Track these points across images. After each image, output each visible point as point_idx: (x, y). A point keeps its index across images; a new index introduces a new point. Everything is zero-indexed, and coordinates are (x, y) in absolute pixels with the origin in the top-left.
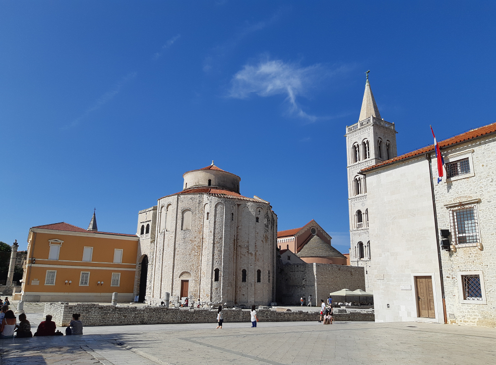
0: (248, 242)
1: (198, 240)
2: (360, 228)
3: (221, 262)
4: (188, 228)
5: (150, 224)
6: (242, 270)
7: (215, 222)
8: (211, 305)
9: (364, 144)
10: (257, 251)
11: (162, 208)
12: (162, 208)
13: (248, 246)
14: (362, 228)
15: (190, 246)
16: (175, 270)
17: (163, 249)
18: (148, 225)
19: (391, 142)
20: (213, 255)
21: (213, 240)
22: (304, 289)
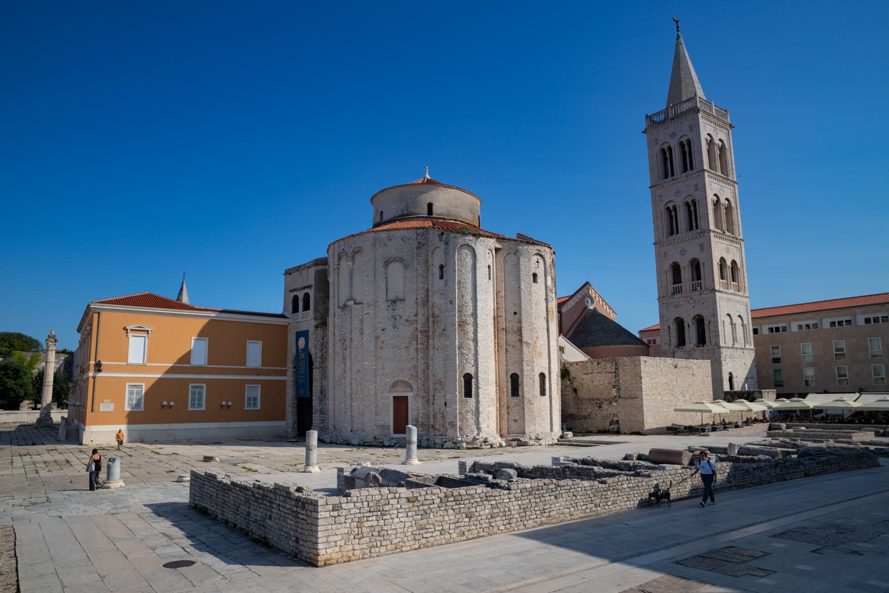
1: (421, 319)
5: (311, 292)
6: (509, 374)
9: (682, 145)
10: (537, 338)
11: (339, 259)
12: (339, 259)
15: (406, 331)
17: (351, 339)
18: (307, 297)
19: (725, 142)
22: (614, 404)
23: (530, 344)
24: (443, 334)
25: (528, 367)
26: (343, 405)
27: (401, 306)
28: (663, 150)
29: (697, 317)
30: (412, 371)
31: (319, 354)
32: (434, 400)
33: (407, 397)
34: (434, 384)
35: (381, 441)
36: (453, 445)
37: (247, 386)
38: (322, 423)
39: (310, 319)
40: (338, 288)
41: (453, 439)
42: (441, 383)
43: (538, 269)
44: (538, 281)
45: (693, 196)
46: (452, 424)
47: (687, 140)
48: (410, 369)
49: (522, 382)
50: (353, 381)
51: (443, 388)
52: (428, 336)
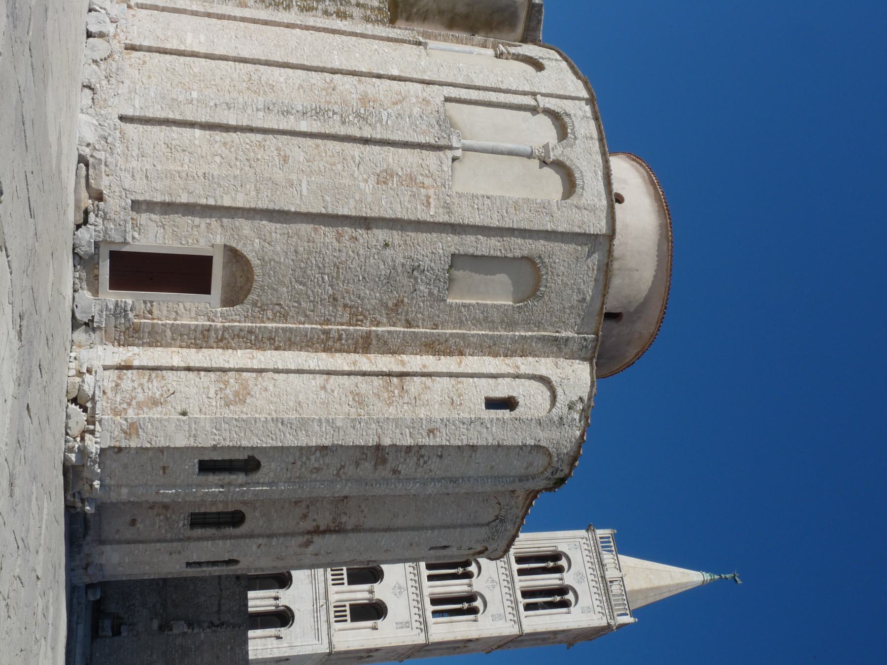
0: (357, 529)
2: (330, 582)
6: (243, 509)
8: (83, 452)
9: (562, 590)
11: (556, 117)
12: (556, 117)
13: (339, 530)
14: (333, 589)
17: (366, 141)
22: (155, 624)
25: (254, 547)
26: (195, 95)
28: (556, 556)
29: (289, 613)
30: (277, 307)
32: (199, 370)
33: (207, 290)
34: (240, 370)
35: (92, 217)
41: (92, 432)
42: (241, 397)
43: (455, 549)
44: (431, 552)
45: (484, 611)
47: (570, 600)
48: (280, 305)
49: (224, 538)
50: (260, 137)
51: (227, 405)
52: (355, 352)
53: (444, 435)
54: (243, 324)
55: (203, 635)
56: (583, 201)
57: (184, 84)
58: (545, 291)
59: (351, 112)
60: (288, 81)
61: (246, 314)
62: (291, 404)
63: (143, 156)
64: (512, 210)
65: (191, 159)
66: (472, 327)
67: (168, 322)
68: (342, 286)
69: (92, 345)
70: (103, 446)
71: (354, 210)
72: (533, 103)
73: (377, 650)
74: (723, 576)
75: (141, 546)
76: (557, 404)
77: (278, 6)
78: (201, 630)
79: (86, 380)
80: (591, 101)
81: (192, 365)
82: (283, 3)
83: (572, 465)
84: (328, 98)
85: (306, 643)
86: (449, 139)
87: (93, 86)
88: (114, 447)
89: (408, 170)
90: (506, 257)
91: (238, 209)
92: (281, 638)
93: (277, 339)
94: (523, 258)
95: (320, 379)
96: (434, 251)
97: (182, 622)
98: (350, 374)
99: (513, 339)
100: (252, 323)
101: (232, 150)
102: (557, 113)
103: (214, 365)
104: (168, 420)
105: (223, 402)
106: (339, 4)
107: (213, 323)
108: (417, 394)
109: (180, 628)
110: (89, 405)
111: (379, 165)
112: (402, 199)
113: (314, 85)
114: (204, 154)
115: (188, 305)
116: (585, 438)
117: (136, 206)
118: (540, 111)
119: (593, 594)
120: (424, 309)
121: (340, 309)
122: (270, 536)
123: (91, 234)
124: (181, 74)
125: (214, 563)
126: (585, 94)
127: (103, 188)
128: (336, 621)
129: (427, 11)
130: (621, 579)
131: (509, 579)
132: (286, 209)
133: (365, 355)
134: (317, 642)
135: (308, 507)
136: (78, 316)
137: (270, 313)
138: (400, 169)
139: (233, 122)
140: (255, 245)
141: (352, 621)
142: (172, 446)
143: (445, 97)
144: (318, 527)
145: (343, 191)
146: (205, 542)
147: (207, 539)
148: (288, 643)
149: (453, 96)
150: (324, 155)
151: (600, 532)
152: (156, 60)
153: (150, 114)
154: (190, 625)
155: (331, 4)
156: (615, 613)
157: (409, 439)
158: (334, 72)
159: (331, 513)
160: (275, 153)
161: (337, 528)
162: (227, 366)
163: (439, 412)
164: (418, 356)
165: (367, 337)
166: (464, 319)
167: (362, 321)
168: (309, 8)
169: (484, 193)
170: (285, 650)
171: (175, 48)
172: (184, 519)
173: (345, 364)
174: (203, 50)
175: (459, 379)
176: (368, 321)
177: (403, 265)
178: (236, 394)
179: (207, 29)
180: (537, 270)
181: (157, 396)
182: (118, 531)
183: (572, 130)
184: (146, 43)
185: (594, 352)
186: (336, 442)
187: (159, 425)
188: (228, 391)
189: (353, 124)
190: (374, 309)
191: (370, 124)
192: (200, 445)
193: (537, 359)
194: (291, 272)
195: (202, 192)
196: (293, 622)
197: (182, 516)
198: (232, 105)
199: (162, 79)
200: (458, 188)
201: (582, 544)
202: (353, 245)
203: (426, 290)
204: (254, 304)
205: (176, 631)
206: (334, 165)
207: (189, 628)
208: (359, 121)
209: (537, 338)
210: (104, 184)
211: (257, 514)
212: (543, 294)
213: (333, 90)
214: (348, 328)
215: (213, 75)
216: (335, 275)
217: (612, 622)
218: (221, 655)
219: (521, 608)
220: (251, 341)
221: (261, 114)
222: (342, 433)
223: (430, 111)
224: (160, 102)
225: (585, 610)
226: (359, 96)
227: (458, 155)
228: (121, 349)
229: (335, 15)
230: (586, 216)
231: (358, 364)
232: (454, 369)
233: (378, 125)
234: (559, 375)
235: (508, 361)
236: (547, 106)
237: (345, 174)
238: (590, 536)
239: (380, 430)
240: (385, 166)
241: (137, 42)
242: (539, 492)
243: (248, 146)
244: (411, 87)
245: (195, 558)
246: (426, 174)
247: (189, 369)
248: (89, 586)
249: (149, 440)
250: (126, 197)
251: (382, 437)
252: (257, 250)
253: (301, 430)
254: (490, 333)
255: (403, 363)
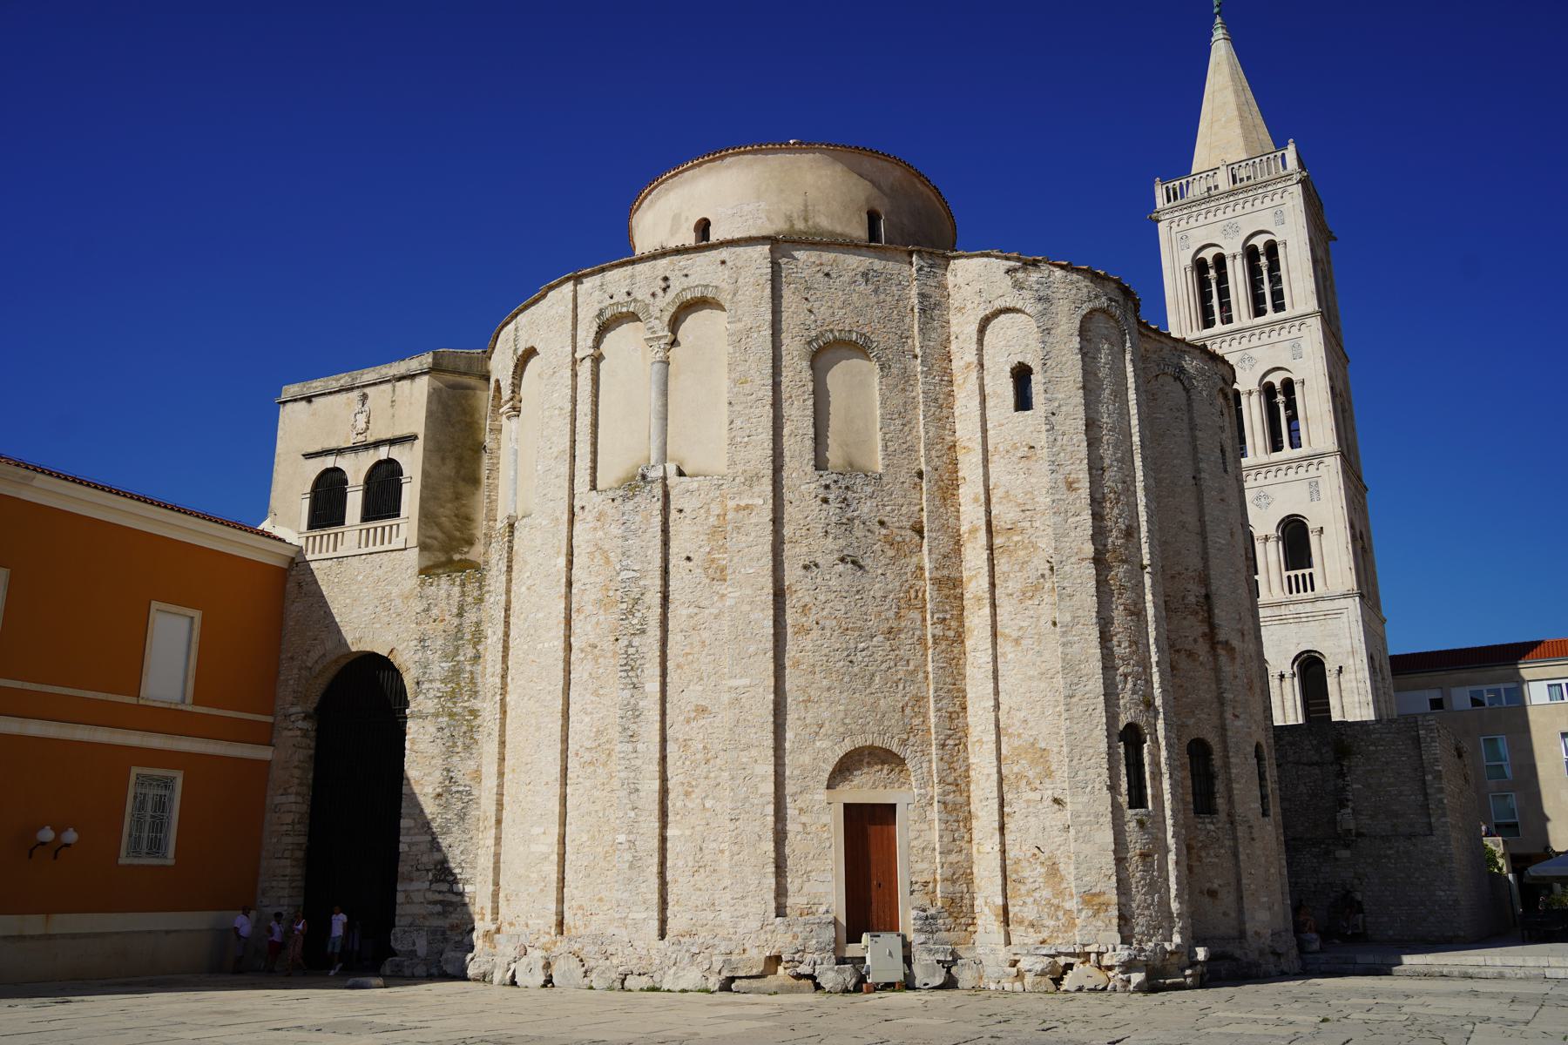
0: (1205, 580)
3: (1149, 682)
4: (861, 461)
5: (411, 461)
6: (1186, 741)
7: (1091, 425)
8: (1128, 966)
9: (1251, 254)
11: (603, 330)
12: (603, 330)
16: (789, 735)
17: (665, 598)
20: (1105, 638)
21: (1094, 538)
22: (1344, 854)
23: (1233, 649)
24: (1037, 588)
25: (1238, 723)
26: (622, 838)
27: (869, 490)
28: (1200, 266)
30: (908, 711)
31: (439, 668)
33: (891, 809)
35: (805, 969)
36: (1099, 978)
37: (135, 771)
38: (444, 914)
39: (398, 543)
40: (595, 425)
43: (1224, 436)
46: (1097, 900)
49: (1227, 765)
51: (1049, 774)
52: (961, 597)
53: (1073, 467)
54: (934, 756)
55: (1355, 786)
56: (724, 285)
57: (607, 852)
58: (857, 333)
59: (627, 622)
60: (589, 710)
61: (918, 754)
62: (1043, 685)
63: (713, 904)
64: (747, 388)
65: (712, 838)
66: (915, 434)
67: (938, 860)
68: (871, 623)
69: (978, 962)
70: (1119, 941)
71: (765, 613)
72: (588, 363)
73: (1352, 527)
74: (1216, 10)
75: (1244, 881)
76: (1018, 307)
77: (473, 727)
78: (1348, 788)
79: (1028, 968)
80: (578, 280)
81: (996, 825)
82: (467, 720)
83: (1105, 278)
84: (609, 655)
85: (1347, 630)
86: (653, 482)
87: (623, 977)
88: (1119, 926)
89: (702, 537)
90: (814, 392)
91: (776, 771)
92: (1341, 667)
93: (951, 709)
94: (812, 367)
95: (1004, 647)
96: (813, 495)
97: (1339, 818)
98: (994, 606)
99: (926, 374)
100: (931, 745)
101: (694, 783)
102: (599, 327)
103: (995, 794)
104: (1077, 855)
105: (1047, 780)
106: (461, 642)
107: (936, 799)
108: (1018, 509)
109: (1346, 819)
110: (1062, 961)
111: (698, 580)
112: (744, 545)
113: (590, 674)
114: (704, 822)
115: (912, 835)
116: (1065, 263)
117: (780, 911)
118: (597, 352)
119: (1255, 209)
120: (894, 505)
121: (903, 624)
122: (1221, 702)
123: (828, 969)
124: (592, 858)
125: (1262, 777)
126: (568, 288)
127: (763, 958)
128: (1313, 589)
129: (456, 516)
130: (1230, 168)
131: (1238, 336)
132: (771, 706)
133: (964, 584)
134: (1345, 615)
135: (1178, 651)
136: (938, 981)
137: (916, 721)
138: (702, 550)
139: (656, 785)
140: (824, 746)
141: (1310, 566)
142: (1113, 847)
143: (591, 490)
144: (1204, 635)
145: (740, 628)
146: (1235, 792)
147: (1229, 790)
148: (1348, 658)
149: (588, 478)
150: (690, 657)
151: (1160, 200)
152: (575, 892)
153: (655, 897)
154: (1342, 804)
155: (462, 654)
156: (1283, 173)
157: (1082, 518)
158: (569, 647)
159: (1185, 618)
160: (693, 724)
161: (1205, 608)
162: (995, 777)
163: (1041, 476)
164: (962, 509)
165: (938, 582)
166: (905, 446)
167: (917, 591)
168: (471, 681)
169: (726, 427)
170: (1359, 662)
171: (556, 868)
172: (1203, 823)
173: (981, 613)
174: (555, 830)
175: (990, 448)
176: (917, 582)
177: (835, 538)
178: (1033, 763)
179: (522, 823)
180: (828, 345)
181: (1043, 870)
182: (1225, 914)
183: (622, 306)
184: (553, 907)
185: (938, 255)
186: (1094, 620)
187: (1085, 865)
188: (1031, 774)
189: (644, 618)
190: (900, 575)
191: (642, 594)
192: (1110, 809)
193: (952, 338)
194: (857, 695)
195: (757, 823)
196: (1316, 652)
197: (1199, 826)
198: (632, 786)
199: (602, 883)
200: (720, 465)
201: (1179, 229)
202: (814, 612)
203: (869, 504)
204: (904, 743)
205: (1352, 826)
206: (704, 642)
207: (1348, 806)
208: (639, 611)
209: (924, 339)
210: (756, 958)
211: (1191, 722)
212: (862, 335)
213: (596, 647)
214: (929, 611)
215: (589, 814)
216: (856, 634)
217: (1297, 177)
218: (1383, 759)
219: (1281, 315)
220: (956, 745)
221: (640, 747)
222: (1080, 613)
223: (614, 511)
224: (637, 884)
225: (1280, 218)
226: (601, 612)
227: (675, 468)
228: (979, 921)
229: (478, 647)
230: (747, 280)
231: (980, 593)
232: (977, 457)
233: (641, 583)
234: (975, 305)
235: (958, 379)
236: (590, 342)
237: (715, 626)
238: (1167, 216)
239: (1073, 560)
240: (699, 571)
241: (553, 919)
242: (1139, 322)
243: (688, 763)
244: (581, 538)
245: (1257, 805)
246: (706, 512)
247: (1002, 828)
248: (1302, 948)
249: (1106, 879)
250: (772, 924)
251: (1082, 556)
252: (831, 743)
253: (1080, 670)
254: (921, 407)
255: (973, 531)
